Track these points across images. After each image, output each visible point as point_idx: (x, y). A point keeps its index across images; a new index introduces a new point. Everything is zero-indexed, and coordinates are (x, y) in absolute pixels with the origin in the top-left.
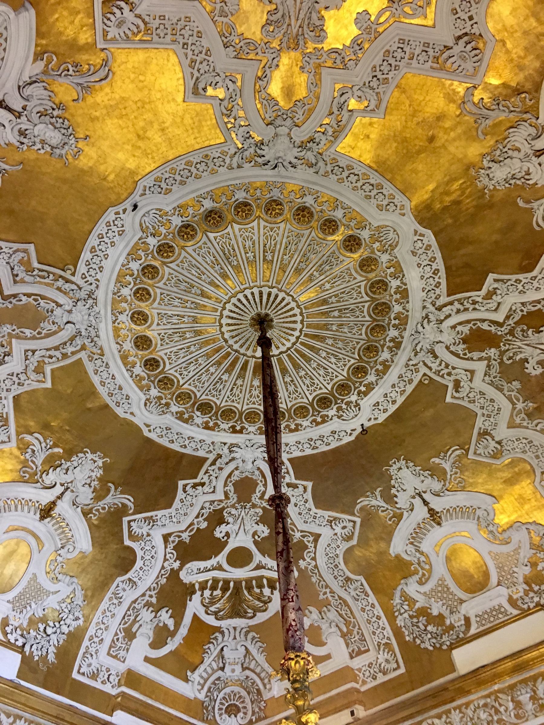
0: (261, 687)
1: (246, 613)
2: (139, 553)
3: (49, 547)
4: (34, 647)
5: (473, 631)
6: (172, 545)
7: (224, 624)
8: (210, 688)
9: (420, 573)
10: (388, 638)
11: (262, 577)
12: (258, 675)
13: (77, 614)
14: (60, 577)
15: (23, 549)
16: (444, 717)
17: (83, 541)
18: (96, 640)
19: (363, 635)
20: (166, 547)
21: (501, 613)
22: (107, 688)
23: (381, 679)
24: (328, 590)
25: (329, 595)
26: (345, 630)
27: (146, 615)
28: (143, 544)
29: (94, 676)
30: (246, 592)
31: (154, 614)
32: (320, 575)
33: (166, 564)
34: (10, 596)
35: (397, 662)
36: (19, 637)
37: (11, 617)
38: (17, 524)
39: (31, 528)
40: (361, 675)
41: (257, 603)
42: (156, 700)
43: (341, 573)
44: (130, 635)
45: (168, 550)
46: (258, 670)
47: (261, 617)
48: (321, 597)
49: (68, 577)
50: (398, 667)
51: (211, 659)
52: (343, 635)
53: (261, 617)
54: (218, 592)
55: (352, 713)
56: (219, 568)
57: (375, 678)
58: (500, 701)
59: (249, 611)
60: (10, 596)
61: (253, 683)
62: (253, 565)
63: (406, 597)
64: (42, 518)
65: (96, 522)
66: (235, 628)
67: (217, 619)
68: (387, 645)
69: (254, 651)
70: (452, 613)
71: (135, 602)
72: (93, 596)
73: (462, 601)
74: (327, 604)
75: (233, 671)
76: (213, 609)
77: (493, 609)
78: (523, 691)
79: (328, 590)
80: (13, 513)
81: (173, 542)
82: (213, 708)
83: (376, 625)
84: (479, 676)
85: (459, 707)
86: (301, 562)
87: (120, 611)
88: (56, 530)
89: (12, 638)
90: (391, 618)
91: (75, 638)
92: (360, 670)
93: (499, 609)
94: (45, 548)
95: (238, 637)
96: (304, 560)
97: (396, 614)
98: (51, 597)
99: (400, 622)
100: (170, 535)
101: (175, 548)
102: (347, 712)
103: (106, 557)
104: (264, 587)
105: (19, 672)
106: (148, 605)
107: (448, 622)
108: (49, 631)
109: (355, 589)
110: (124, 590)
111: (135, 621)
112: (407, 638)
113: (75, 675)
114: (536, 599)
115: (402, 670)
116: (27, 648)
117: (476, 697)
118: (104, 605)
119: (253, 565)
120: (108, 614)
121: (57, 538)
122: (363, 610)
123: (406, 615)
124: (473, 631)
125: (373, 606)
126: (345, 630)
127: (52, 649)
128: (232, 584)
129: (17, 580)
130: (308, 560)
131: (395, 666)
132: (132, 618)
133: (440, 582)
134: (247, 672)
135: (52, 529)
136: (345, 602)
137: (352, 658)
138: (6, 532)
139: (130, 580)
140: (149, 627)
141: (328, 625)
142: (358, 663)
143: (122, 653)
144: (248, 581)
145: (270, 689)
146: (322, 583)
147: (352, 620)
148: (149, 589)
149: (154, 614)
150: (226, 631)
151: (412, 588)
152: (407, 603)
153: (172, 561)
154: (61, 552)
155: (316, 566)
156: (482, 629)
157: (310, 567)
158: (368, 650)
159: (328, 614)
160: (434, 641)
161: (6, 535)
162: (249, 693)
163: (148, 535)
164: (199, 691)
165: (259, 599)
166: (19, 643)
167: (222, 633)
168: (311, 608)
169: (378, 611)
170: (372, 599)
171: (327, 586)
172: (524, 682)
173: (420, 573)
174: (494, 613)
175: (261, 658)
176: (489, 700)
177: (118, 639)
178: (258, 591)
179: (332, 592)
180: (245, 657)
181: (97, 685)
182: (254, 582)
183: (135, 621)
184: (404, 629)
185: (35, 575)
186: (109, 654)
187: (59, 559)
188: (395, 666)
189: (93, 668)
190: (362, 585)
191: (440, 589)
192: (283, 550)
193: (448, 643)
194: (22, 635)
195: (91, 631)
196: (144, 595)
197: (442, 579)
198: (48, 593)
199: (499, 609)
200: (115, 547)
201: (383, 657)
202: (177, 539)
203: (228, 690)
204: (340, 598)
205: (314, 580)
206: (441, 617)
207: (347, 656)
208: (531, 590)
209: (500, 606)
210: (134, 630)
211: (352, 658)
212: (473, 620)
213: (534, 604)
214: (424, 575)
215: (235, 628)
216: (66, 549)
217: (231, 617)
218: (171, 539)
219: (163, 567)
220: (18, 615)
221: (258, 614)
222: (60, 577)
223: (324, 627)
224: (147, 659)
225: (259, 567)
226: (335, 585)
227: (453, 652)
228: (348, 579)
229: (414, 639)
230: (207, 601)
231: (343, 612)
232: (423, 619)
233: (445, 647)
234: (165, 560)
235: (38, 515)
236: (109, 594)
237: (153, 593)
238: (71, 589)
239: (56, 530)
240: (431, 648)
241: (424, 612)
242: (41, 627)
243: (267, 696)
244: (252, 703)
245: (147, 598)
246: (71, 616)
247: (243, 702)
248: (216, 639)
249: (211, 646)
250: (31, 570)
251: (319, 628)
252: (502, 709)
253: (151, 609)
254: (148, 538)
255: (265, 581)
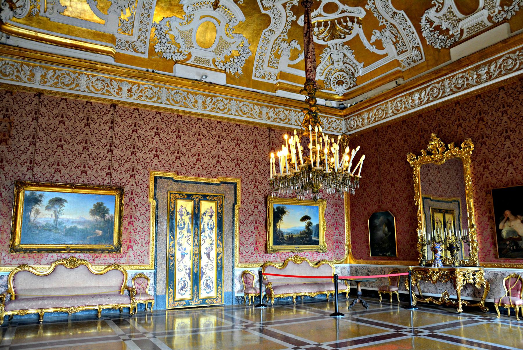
0: (353, 71)
1: (341, 36)
2: (272, 16)
3: (223, 23)
4: (231, 69)
5: (464, 37)
6: (289, 9)
7: (329, 43)
8: (327, 74)
9: (437, 6)
10: (418, 44)
11: (346, 17)
12: (352, 66)
13: (247, 51)
14: (234, 35)
15: (211, 26)
16: (441, 83)
17: (240, 16)
18: (260, 61)
19: (404, 42)
20: (286, 10)
21: (482, 26)
22: (271, 81)
23: (413, 64)
24: (384, 20)
25: (384, 23)
26: (395, 41)
27: (284, 45)
28: (272, 11)
29: (264, 77)
30: (338, 25)
31: (288, 44)
32: (379, 12)
33: (288, 19)
34: (212, 48)
35: (421, 56)
36: (222, 66)
37: (216, 58)
38: (204, 14)
39: (211, 15)
40: (403, 63)
41: (346, 30)
42: (298, 83)
43: (391, 10)
44: (278, 56)
45: (287, 11)
46: (351, 63)
47: (349, 38)
48: (381, 24)
49: (238, 35)
50: (422, 58)
51: (325, 60)
52: (394, 43)
53: (349, 38)
54: (322, 28)
55: (396, 82)
56: (320, 15)
57: (409, 64)
58: (470, 74)
59: (342, 35)
60: (212, 48)
61: (349, 70)
62: (339, 11)
63: (427, 20)
64: (215, 9)
65: (243, 5)
66: (336, 44)
67: (324, 41)
68: (418, 48)
69: (348, 54)
70: (453, 27)
71: (276, 40)
72: (253, 41)
73: (460, 20)
74: (384, 27)
75: (338, 65)
76: (321, 36)
77: (478, 24)
78: (483, 69)
79: (384, 20)
80: (200, 10)
81: (289, 7)
82: (330, 83)
83: (411, 37)
84: (460, 63)
85: (449, 78)
86: (366, 6)
87: (270, 46)
88: (224, 13)
89: (219, 67)
90: (420, 33)
91: (250, 62)
92: (402, 61)
93: (481, 24)
94: (221, 23)
95: (338, 48)
96: (368, 5)
97: (422, 30)
98: (232, 45)
99: (424, 34)
100: (286, 3)
101: (291, 10)
102: (394, 82)
103: (254, 21)
104: (348, 22)
105: (226, 80)
106: (284, 40)
107: (451, 33)
108: (236, 61)
109: (399, 18)
110: (269, 35)
111: (278, 49)
112: (428, 43)
113: (254, 78)
114: (504, 16)
115: (424, 60)
116: (227, 70)
117: (458, 73)
118: (260, 44)
119: (339, 11)
120: (263, 48)
121: (226, 17)
122: (404, 29)
123: (428, 31)
124: (464, 37)
125: (410, 27)
126: (395, 41)
127: (239, 69)
128: (329, 23)
129: (213, 41)
130: (371, 4)
131: (420, 58)
132: (277, 48)
133: (449, 10)
134: (346, 65)
135: (222, 13)
136: (394, 25)
137: (398, 55)
138: (200, 19)
139: (270, 30)
140: (287, 51)
141: (385, 39)
142: (401, 58)
143: (275, 65)
144: (339, 19)
145: (358, 72)
146: (380, 16)
147: (399, 35)
148: (282, 32)
149: (288, 44)
150: (331, 46)
151: (431, 14)
152: (429, 23)
153: (291, 16)
154: (230, 23)
155: (376, 8)
156: (469, 35)
157: (372, 8)
158: (407, 51)
159: (385, 33)
160: (442, 44)
161: (201, 21)
162: (348, 74)
163: (274, 6)
164: (321, 76)
165: (346, 29)
166: (223, 68)
167: (329, 47)
168: (376, 31)
169: (413, 29)
170: (409, 23)
171: (383, 18)
172: (484, 64)
173: (437, 6)
174: (478, 26)
175: (352, 58)
176: (464, 74)
177: (272, 59)
178: (345, 24)
179: (386, 21)
180: (344, 57)
181: (266, 81)
182: (342, 20)
183: (278, 49)
184: (426, 38)
185: (221, 36)
186: (268, 66)
187: (230, 27)
188: (420, 58)
189: (262, 73)
190: (403, 16)
191: (448, 14)
192: (307, 32)
193: (449, 45)
194: (223, 65)
195: (257, 58)
196: (280, 36)
197: (450, 8)
198: (230, 44)
199: (481, 24)
200: (258, 15)
201: (414, 53)
202: (291, 5)
203: (337, 74)
204: (391, 24)
205: (375, 15)
206: (448, 30)
207: (396, 54)
208: (503, 10)
209: (482, 22)
210: (279, 53)
211: (398, 55)
212: (465, 31)
213: (502, 19)
214: (439, 6)
215: (336, 44)
216: (232, 21)
217: (331, 39)
218: (287, 5)
219: (287, 21)
220: (219, 57)
221: (347, 36)
222: (234, 35)
223: (383, 40)
224: (289, 66)
225: (343, 12)
226: (388, 17)
227: (451, 49)
228: (395, 13)
229: (432, 43)
230: (317, 33)
231: (393, 32)
232: (437, 32)
233: (447, 47)
234: (287, 17)
235: (212, 8)
236: (261, 39)
237: (285, 34)
238: (241, 39)
239: (224, 13)
240: (440, 48)
241: (438, 28)
242: (232, 60)
243: (356, 75)
244: (350, 79)
245: (282, 37)
246: (244, 52)
247: (345, 79)
248: (326, 50)
249: (324, 54)
250: (219, 34)
251: (381, 40)
252: (470, 78)
253: (286, 42)
254: (274, 7)
255: (348, 19)
